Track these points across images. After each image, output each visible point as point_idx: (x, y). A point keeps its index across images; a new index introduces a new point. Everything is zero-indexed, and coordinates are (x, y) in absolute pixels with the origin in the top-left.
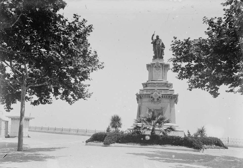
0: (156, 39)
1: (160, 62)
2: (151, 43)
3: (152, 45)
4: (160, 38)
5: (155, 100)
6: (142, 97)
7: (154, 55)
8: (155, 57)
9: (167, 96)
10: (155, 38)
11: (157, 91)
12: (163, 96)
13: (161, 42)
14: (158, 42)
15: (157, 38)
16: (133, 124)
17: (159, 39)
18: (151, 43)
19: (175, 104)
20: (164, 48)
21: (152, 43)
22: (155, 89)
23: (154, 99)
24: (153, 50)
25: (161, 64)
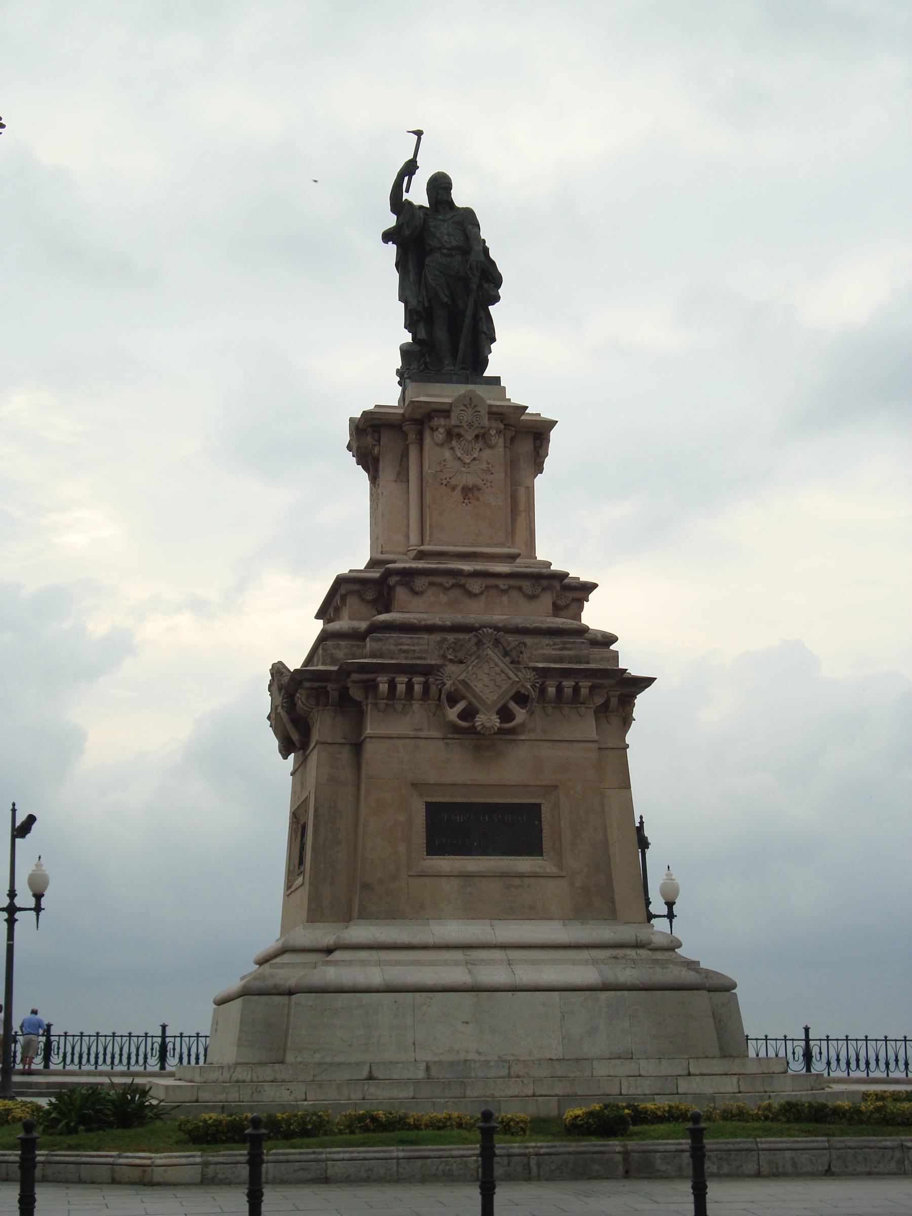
3: (391, 249)
4: (460, 197)
5: (481, 720)
6: (356, 693)
7: (408, 337)
8: (417, 363)
10: (418, 194)
11: (497, 642)
12: (542, 691)
21: (387, 237)
24: (402, 298)
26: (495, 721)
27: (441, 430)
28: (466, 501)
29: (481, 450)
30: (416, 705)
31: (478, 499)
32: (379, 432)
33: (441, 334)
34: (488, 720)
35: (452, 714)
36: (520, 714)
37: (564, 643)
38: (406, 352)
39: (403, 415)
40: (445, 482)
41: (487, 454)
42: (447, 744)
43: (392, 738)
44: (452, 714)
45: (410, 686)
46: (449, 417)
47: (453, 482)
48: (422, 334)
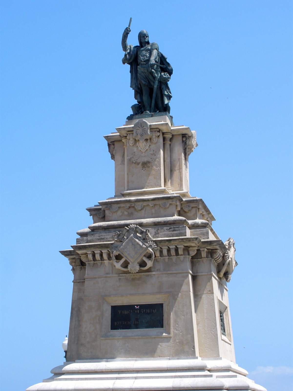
0: (139, 45)
1: (149, 124)
2: (124, 63)
6: (84, 259)
7: (136, 102)
9: (177, 250)
10: (133, 41)
13: (155, 52)
14: (144, 52)
15: (141, 43)
16: (52, 372)
17: (148, 43)
18: (124, 63)
19: (68, 259)
20: (170, 73)
22: (127, 225)
23: (126, 264)
25: (152, 129)
26: (138, 268)
27: (131, 139)
28: (144, 169)
29: (150, 145)
30: (106, 262)
31: (149, 167)
32: (114, 145)
33: (145, 98)
34: (134, 267)
35: (118, 265)
36: (150, 264)
37: (174, 228)
38: (134, 107)
39: (120, 135)
40: (134, 162)
41: (153, 146)
42: (120, 279)
43: (95, 278)
44: (118, 265)
45: (101, 255)
46: (133, 134)
47: (138, 161)
48: (139, 100)
